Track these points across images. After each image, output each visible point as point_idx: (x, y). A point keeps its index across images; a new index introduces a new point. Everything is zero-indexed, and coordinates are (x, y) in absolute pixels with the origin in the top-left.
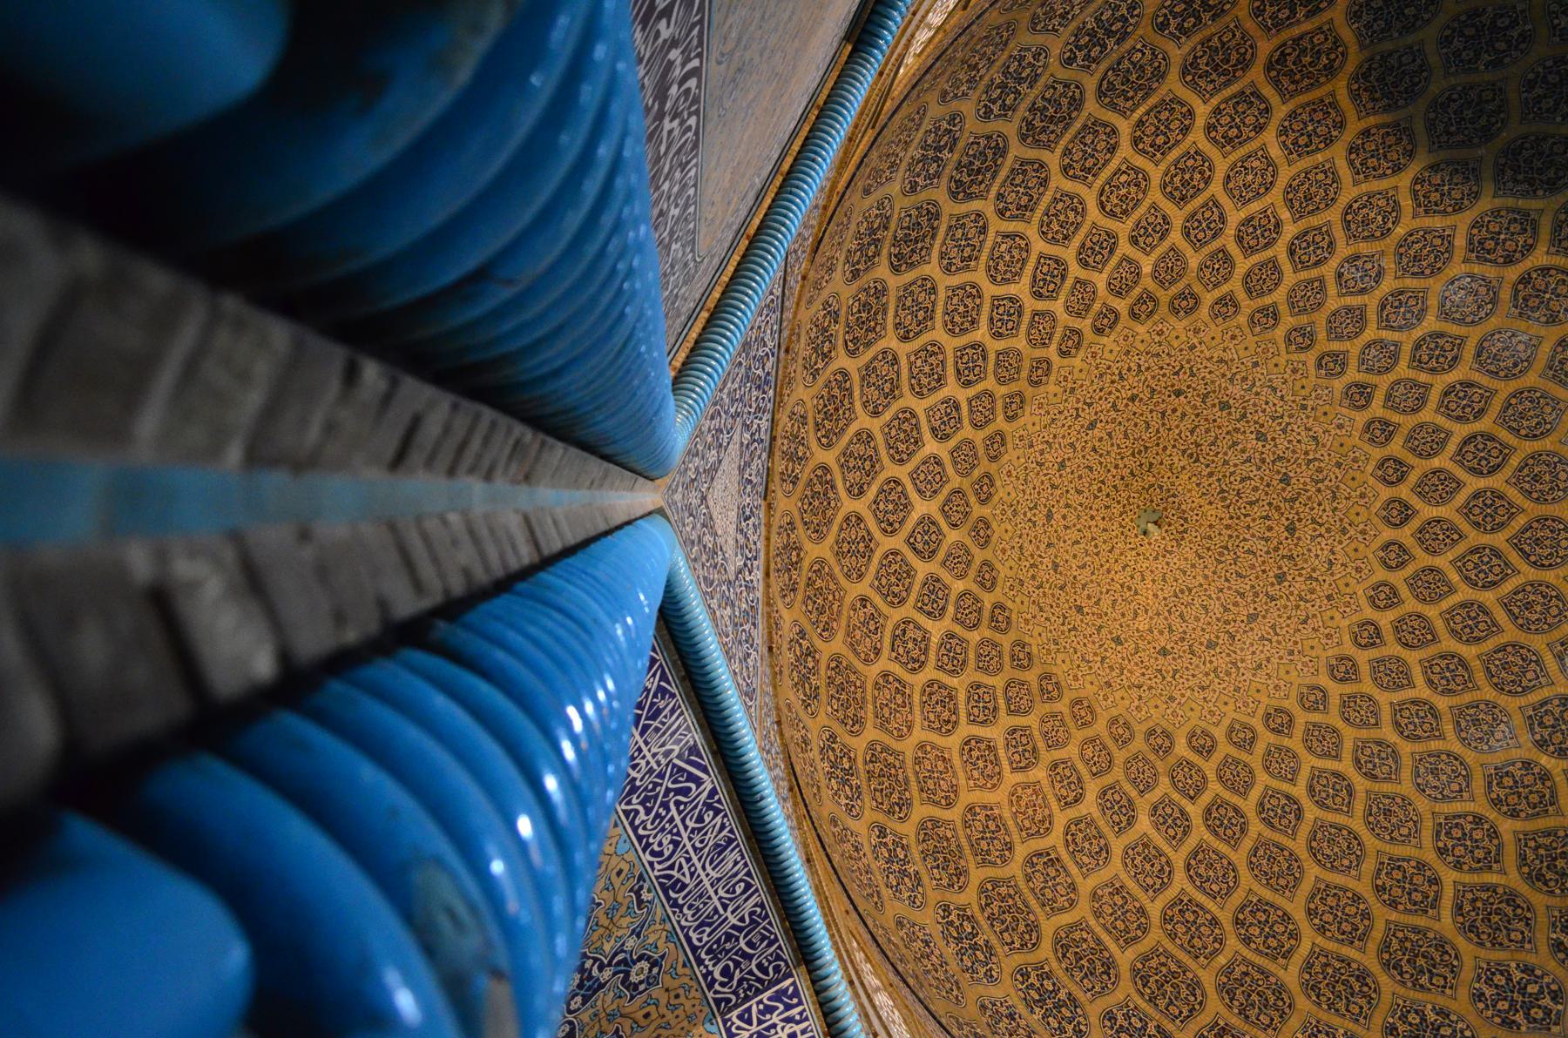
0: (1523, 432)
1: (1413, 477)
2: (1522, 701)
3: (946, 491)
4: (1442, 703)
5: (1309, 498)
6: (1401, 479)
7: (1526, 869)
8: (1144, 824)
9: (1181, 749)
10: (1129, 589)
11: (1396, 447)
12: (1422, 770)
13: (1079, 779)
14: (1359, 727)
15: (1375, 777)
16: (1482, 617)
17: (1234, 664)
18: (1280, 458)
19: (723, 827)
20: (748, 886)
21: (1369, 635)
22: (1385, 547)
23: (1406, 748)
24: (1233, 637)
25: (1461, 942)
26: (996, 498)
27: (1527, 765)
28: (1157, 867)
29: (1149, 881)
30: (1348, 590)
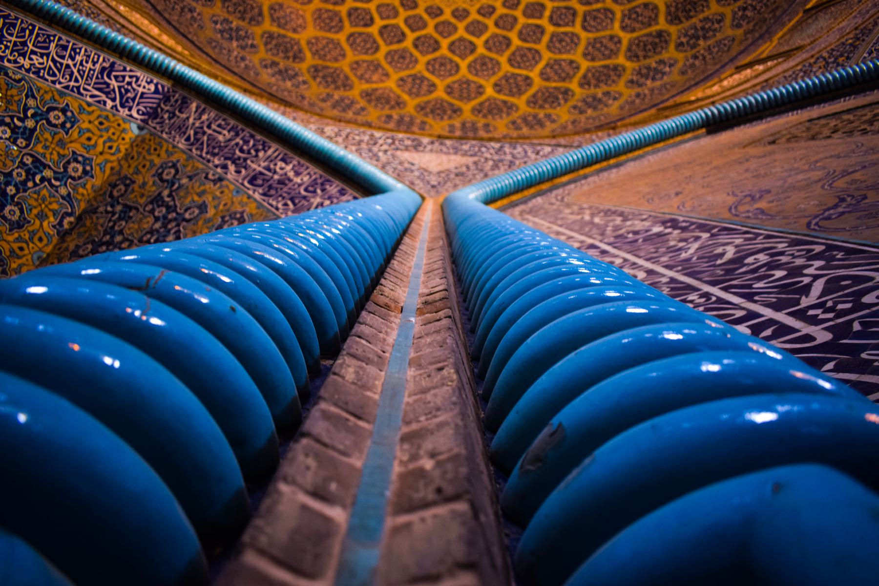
4: (481, 50)
16: (539, 35)
27: (481, 86)
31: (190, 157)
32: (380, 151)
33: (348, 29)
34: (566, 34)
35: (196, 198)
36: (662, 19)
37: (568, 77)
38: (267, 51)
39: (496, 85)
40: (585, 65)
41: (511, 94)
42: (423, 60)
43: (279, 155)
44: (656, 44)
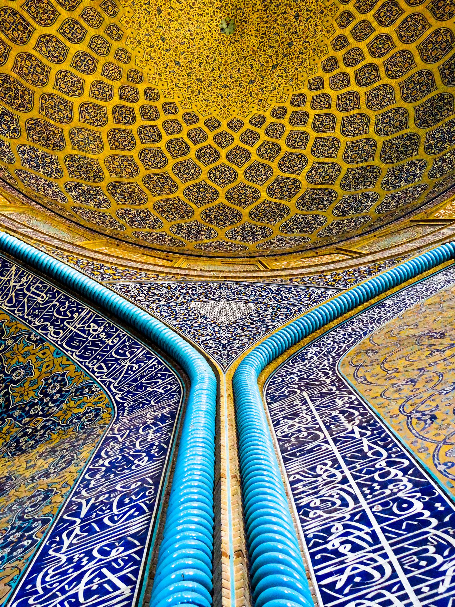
0: (390, 73)
1: (335, 72)
4: (255, 157)
5: (292, 58)
6: (330, 71)
9: (141, 87)
10: (191, 35)
11: (339, 55)
12: (219, 169)
13: (81, 39)
14: (216, 143)
17: (199, 92)
18: (296, 33)
21: (258, 121)
22: (298, 95)
24: (210, 85)
27: (256, 191)
28: (74, 89)
30: (270, 102)
31: (14, 319)
32: (176, 306)
33: (140, 146)
34: (327, 139)
35: (21, 359)
36: (411, 122)
37: (330, 180)
38: (70, 173)
39: (269, 189)
40: (345, 167)
41: (283, 197)
42: (205, 169)
43: (91, 316)
44: (407, 147)
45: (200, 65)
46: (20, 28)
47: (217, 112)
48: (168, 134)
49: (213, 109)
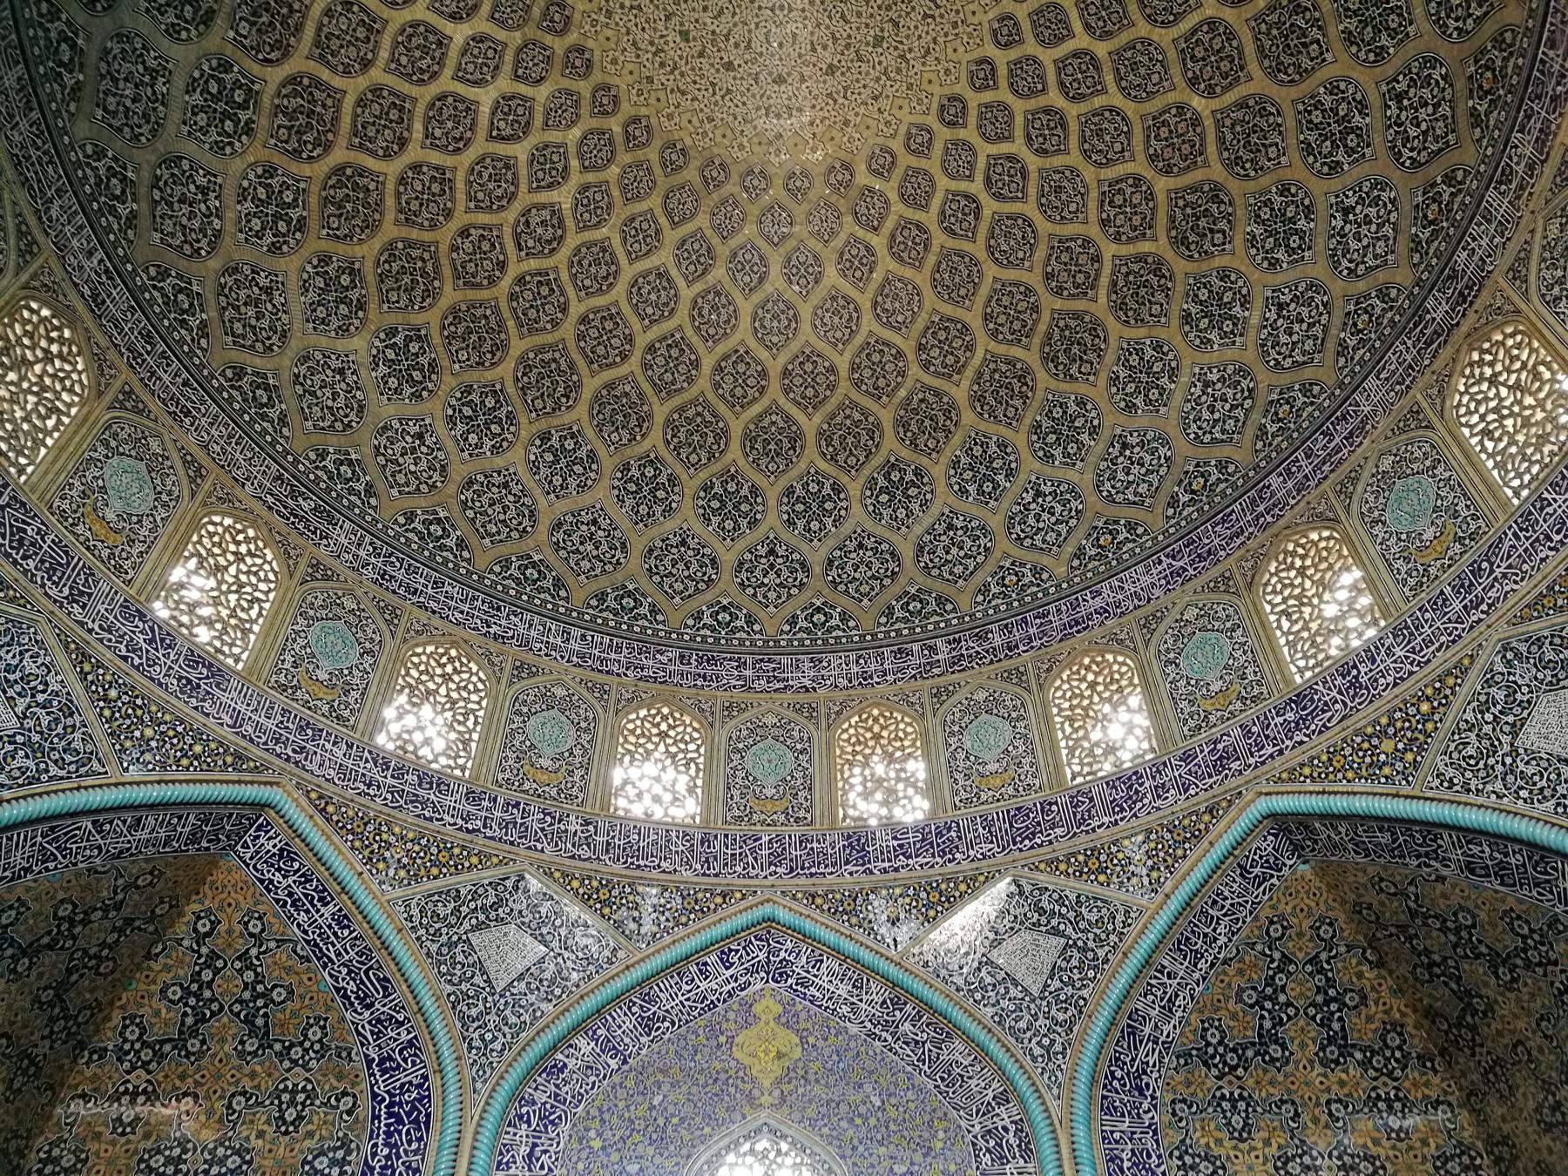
2: (1175, 32)
3: (509, 57)
4: (1101, 49)
7: (1174, 233)
8: (832, 276)
9: (863, 178)
12: (1088, 134)
13: (761, 258)
14: (1028, 97)
15: (1046, 152)
17: (902, 57)
19: (124, 822)
20: (180, 818)
23: (1073, 111)
24: (896, 25)
25: (1111, 322)
26: (577, 16)
27: (1181, 108)
29: (839, 335)
45: (847, 22)
46: (741, 368)
47: (961, 49)
48: (970, 178)
49: (950, 51)
